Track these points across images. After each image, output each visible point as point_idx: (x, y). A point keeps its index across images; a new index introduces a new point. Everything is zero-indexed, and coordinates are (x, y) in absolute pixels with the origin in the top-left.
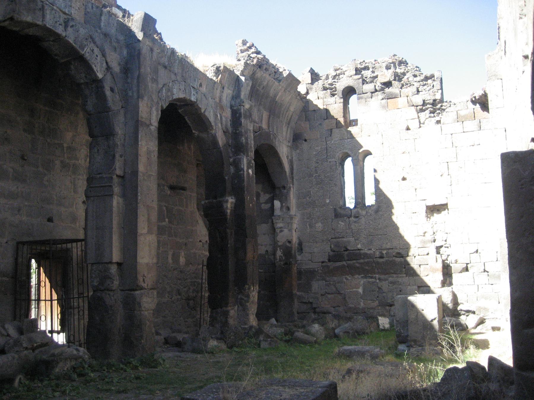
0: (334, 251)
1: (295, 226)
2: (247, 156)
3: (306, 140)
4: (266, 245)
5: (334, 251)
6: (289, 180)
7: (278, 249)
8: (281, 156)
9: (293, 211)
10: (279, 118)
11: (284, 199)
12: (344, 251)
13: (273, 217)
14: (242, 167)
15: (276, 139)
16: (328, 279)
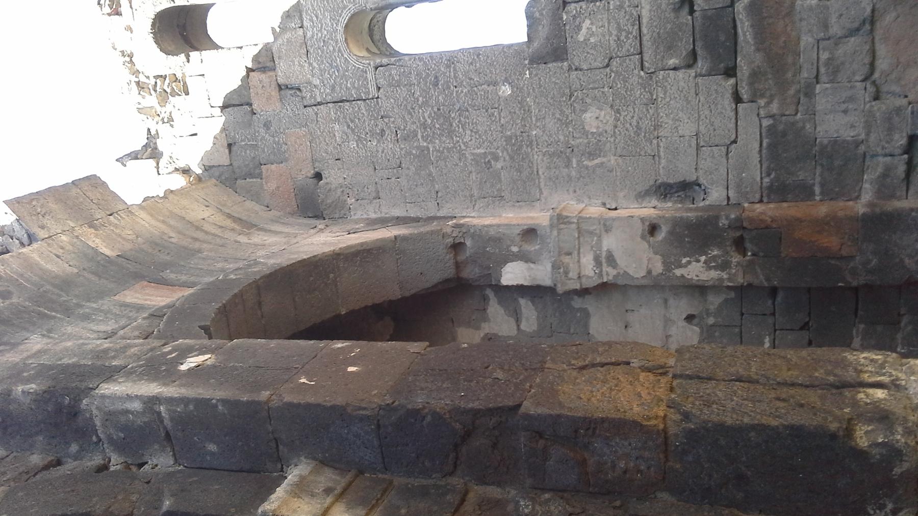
0: (694, 55)
1: (595, 210)
2: (110, 374)
3: (318, 176)
4: (667, 322)
5: (694, 55)
6: (434, 226)
7: (678, 272)
8: (327, 249)
9: (539, 217)
10: (199, 251)
11: (496, 249)
12: (692, 12)
13: (560, 289)
14: (136, 406)
15: (256, 263)
16: (806, 74)
